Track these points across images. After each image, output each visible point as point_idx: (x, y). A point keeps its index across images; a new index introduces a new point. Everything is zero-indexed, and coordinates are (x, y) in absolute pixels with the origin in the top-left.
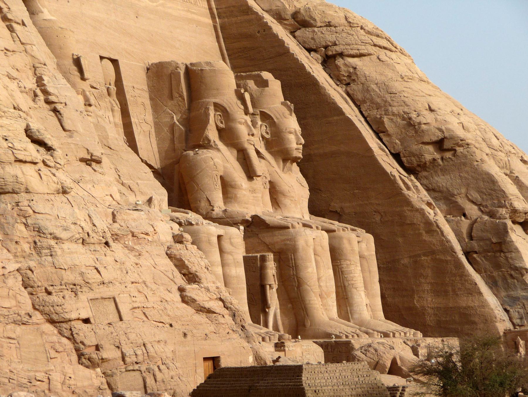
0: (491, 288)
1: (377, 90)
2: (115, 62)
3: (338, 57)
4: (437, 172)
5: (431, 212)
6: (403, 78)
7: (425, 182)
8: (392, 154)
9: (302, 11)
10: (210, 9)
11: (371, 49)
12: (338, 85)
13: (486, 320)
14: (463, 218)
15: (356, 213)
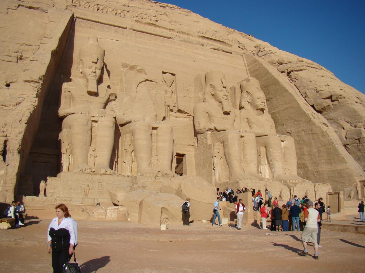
0: (357, 161)
1: (305, 81)
2: (174, 75)
3: (292, 72)
4: (331, 111)
5: (327, 128)
6: (318, 76)
7: (326, 116)
8: (311, 106)
9: (280, 59)
10: (245, 64)
11: (305, 68)
12: (291, 83)
13: (350, 175)
14: (343, 130)
15: (296, 132)
